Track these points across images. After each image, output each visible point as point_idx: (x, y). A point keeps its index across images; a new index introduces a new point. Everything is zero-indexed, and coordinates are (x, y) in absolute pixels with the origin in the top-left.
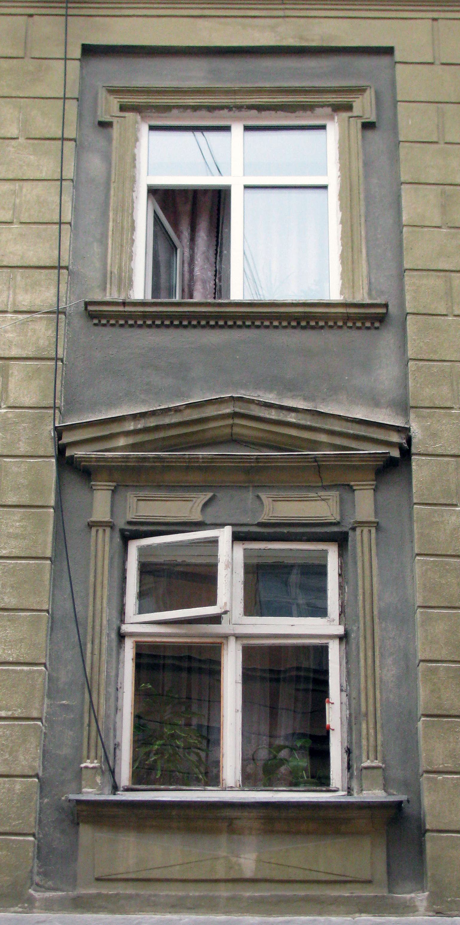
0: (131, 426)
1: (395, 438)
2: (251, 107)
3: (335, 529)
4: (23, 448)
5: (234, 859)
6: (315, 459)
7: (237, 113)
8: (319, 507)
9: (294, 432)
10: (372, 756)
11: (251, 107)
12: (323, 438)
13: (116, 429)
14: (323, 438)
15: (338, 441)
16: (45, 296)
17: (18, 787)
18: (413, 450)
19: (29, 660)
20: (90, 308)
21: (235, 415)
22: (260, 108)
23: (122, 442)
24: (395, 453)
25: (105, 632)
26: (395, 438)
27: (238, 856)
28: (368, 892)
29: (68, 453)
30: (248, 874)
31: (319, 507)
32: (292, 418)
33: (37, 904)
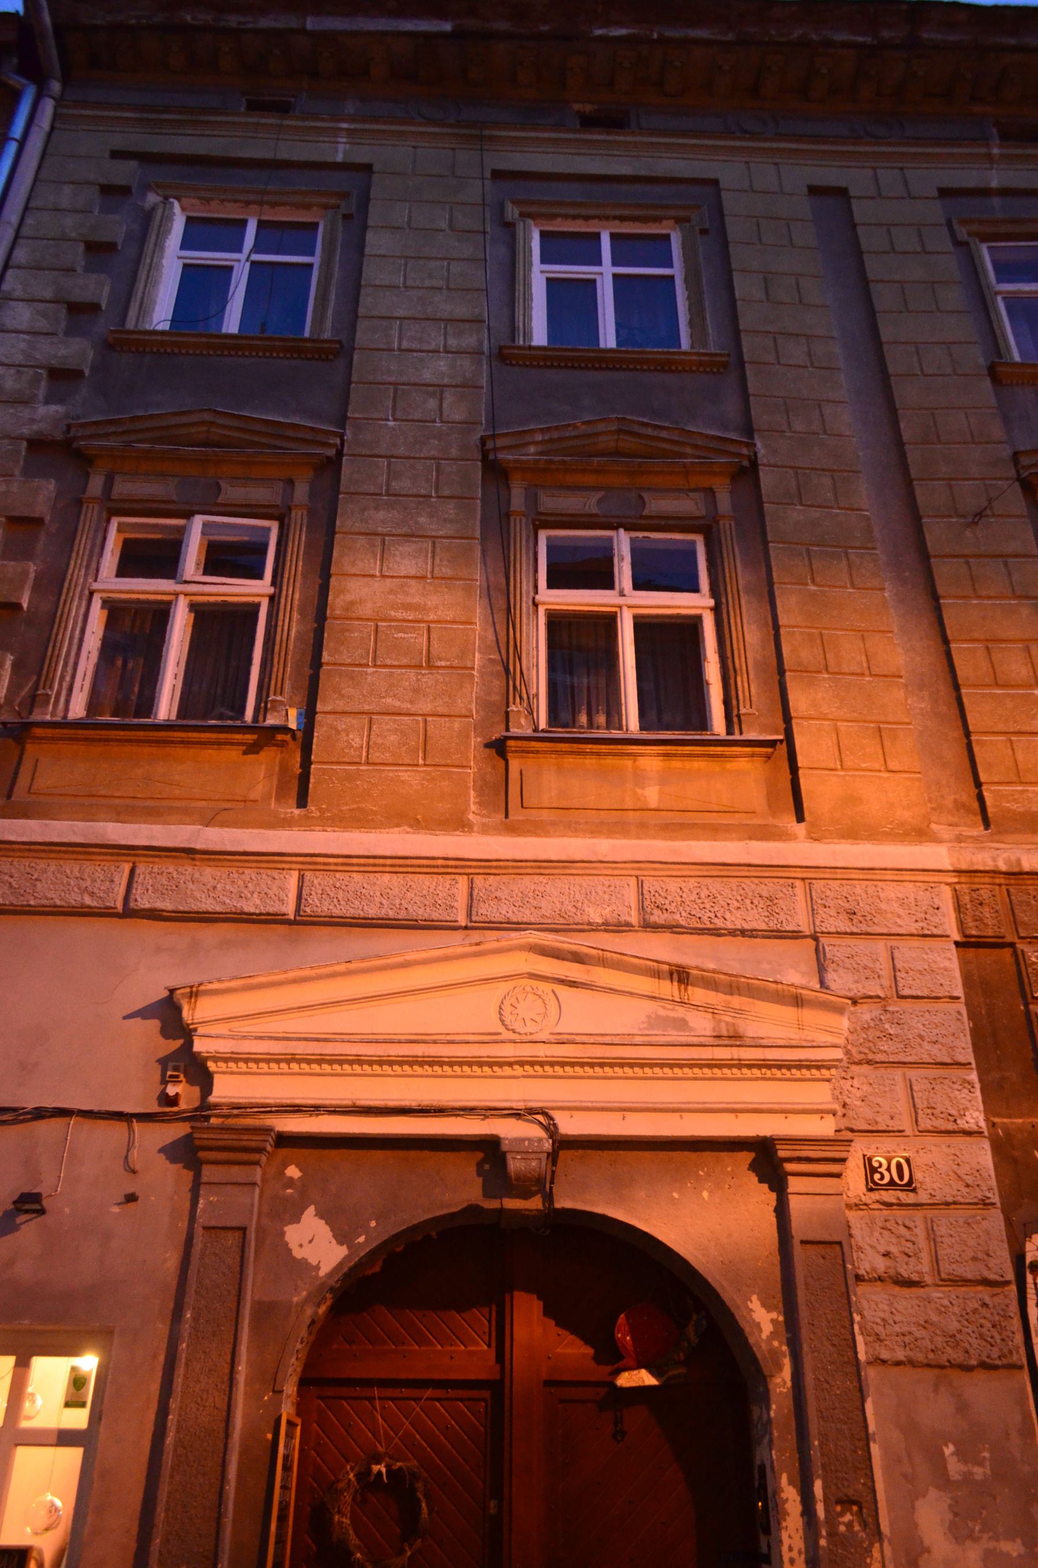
0: (539, 437)
2: (615, 218)
3: (702, 522)
4: (454, 452)
5: (639, 791)
6: (685, 466)
7: (605, 223)
9: (664, 446)
10: (748, 706)
16: (470, 341)
17: (456, 726)
18: (759, 462)
19: (463, 619)
20: (506, 351)
23: (532, 449)
25: (524, 599)
26: (745, 451)
27: (643, 788)
29: (491, 457)
30: (653, 804)
32: (664, 434)
33: (475, 829)
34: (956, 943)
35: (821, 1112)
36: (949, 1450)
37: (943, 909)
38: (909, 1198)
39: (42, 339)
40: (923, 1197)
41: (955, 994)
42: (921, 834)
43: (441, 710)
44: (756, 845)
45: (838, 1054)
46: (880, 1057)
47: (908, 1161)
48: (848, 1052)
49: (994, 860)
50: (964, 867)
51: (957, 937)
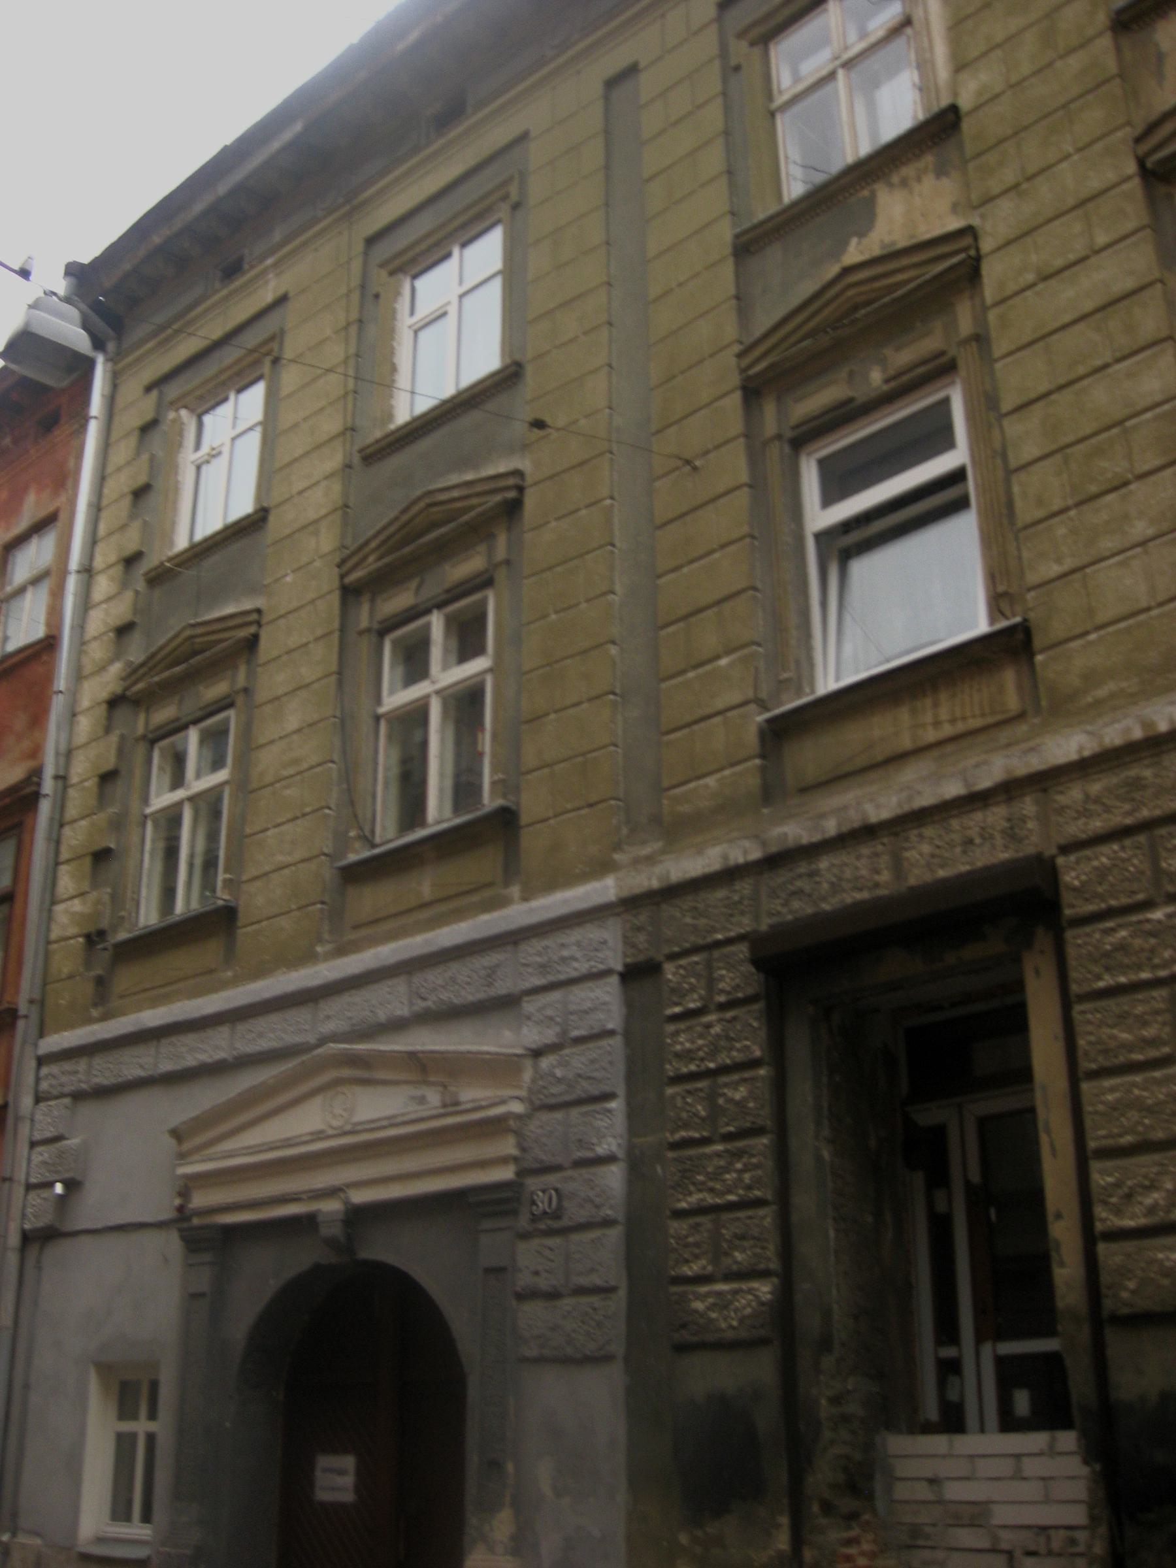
0: (373, 544)
1: (511, 481)
8: (469, 565)
9: (459, 505)
11: (457, 230)
13: (366, 550)
14: (474, 501)
23: (371, 559)
24: (512, 494)
28: (487, 893)
31: (469, 565)
35: (504, 1160)
37: (611, 943)
38: (556, 1225)
40: (565, 1222)
41: (610, 1026)
42: (603, 867)
44: (486, 917)
45: (517, 1108)
46: (552, 1101)
47: (556, 1190)
48: (531, 1102)
50: (626, 893)
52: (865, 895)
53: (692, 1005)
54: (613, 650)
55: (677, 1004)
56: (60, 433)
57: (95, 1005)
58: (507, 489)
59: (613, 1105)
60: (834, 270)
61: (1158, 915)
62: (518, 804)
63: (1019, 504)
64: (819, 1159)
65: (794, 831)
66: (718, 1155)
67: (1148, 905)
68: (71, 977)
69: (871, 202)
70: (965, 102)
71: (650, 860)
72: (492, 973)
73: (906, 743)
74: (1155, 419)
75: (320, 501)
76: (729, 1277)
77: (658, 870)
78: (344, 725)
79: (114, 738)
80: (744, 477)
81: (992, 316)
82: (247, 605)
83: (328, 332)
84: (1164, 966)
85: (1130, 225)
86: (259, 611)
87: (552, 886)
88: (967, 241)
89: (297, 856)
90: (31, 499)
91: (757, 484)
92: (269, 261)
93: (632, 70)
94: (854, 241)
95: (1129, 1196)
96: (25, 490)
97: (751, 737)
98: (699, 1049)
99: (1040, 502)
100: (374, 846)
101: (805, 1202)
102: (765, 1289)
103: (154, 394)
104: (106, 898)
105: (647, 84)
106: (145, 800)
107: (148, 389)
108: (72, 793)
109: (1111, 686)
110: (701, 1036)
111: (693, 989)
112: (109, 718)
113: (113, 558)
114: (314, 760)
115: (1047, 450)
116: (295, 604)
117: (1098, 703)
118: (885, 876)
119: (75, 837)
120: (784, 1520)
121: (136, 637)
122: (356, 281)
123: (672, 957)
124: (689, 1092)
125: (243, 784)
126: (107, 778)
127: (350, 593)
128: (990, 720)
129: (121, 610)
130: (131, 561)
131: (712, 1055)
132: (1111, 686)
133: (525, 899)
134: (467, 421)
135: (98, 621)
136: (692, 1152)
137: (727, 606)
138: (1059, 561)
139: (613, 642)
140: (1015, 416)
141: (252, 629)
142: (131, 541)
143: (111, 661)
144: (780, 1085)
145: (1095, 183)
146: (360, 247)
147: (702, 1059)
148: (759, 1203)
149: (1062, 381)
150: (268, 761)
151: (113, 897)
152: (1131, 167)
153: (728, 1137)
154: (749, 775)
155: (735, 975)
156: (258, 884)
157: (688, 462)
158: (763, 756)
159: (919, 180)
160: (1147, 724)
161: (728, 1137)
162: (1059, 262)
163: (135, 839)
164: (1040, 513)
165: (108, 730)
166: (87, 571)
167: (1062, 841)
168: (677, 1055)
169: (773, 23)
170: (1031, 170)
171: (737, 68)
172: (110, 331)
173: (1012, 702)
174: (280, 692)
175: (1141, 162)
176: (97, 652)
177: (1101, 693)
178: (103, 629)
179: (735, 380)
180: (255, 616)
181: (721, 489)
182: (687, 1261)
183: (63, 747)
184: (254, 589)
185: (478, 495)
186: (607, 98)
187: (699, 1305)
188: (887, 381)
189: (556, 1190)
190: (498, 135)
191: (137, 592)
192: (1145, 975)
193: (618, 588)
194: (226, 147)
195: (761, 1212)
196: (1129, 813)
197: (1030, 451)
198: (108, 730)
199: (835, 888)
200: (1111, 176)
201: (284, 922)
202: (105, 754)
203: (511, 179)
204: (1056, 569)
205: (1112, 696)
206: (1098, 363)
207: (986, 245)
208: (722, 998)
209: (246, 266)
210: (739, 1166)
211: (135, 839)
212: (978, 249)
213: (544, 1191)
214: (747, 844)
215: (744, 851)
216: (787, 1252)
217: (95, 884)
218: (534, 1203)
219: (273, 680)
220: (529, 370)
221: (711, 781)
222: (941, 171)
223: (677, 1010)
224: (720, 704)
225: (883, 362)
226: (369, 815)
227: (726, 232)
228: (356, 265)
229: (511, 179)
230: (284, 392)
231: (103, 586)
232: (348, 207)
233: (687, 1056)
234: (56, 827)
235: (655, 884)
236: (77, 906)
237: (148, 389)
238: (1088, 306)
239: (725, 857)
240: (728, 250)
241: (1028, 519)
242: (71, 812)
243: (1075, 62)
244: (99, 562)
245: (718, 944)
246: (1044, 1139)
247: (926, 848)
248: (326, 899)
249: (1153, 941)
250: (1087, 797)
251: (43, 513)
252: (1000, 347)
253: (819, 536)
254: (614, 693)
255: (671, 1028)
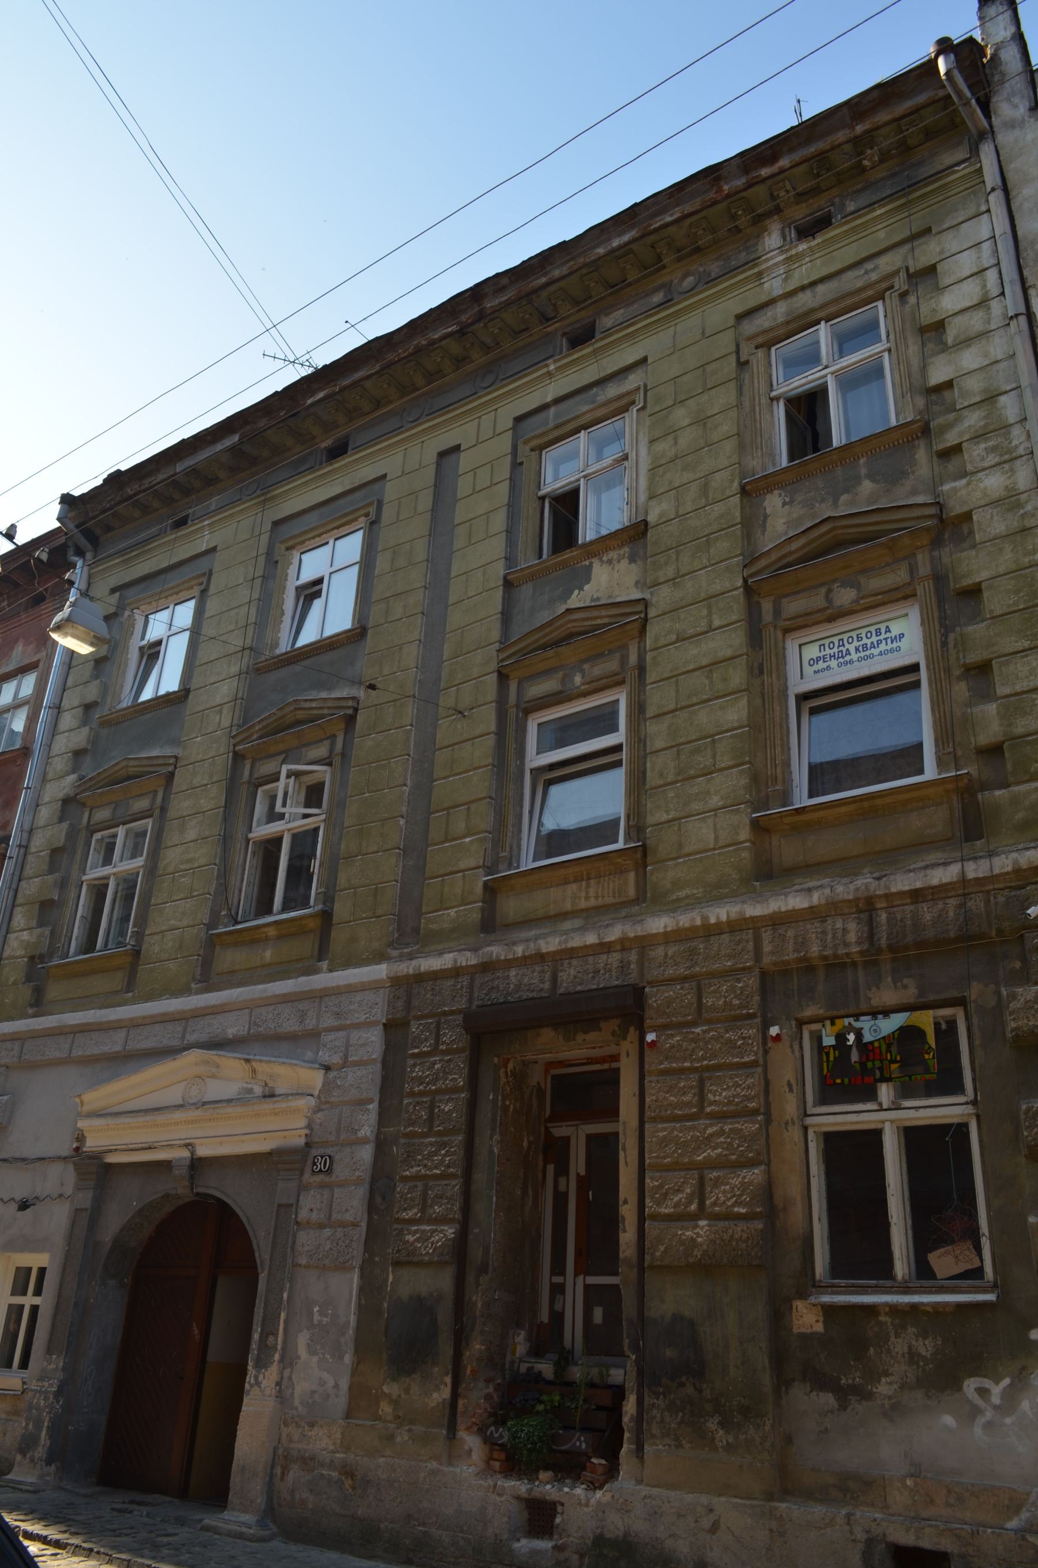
1: (350, 703)
2: (333, 529)
9: (315, 712)
12: (325, 711)
15: (331, 712)
16: (235, 669)
21: (296, 709)
22: (337, 528)
24: (350, 712)
34: (384, 1025)
36: (316, 1309)
39: (73, 733)
42: (380, 957)
43: (191, 923)
47: (330, 1157)
49: (408, 968)
51: (384, 1021)
52: (534, 995)
53: (425, 1049)
54: (402, 822)
55: (415, 1047)
56: (45, 607)
57: (31, 1006)
58: (348, 707)
59: (371, 1106)
60: (562, 609)
61: (698, 1030)
62: (332, 909)
63: (648, 774)
64: (491, 1152)
65: (496, 951)
66: (431, 1144)
67: (694, 1024)
68: (15, 983)
69: (590, 567)
70: (652, 518)
71: (411, 957)
72: (303, 1016)
73: (568, 906)
74: (731, 737)
75: (225, 691)
76: (430, 1221)
77: (414, 963)
78: (226, 841)
79: (65, 825)
80: (493, 727)
81: (649, 657)
82: (168, 751)
83: (241, 580)
84: (698, 1060)
85: (735, 618)
86: (176, 757)
87: (348, 964)
88: (640, 607)
89: (185, 923)
90: (19, 648)
91: (501, 733)
92: (206, 523)
93: (457, 448)
94: (576, 592)
95: (666, 1194)
96: (16, 641)
97: (479, 889)
98: (427, 1076)
99: (661, 775)
100: (237, 923)
101: (480, 1177)
102: (450, 1231)
103: (117, 594)
104: (47, 933)
105: (465, 461)
106: (84, 872)
107: (113, 591)
108: (30, 858)
109: (687, 891)
110: (428, 1069)
111: (426, 1040)
112: (63, 811)
113: (76, 703)
114: (202, 861)
115: (669, 745)
116: (200, 757)
117: (678, 900)
118: (547, 985)
119: (30, 888)
120: (448, 1380)
121: (88, 760)
122: (262, 550)
123: (418, 1018)
124: (418, 1103)
125: (152, 869)
126: (55, 852)
127: (238, 757)
128: (617, 900)
129: (80, 738)
130: (88, 708)
131: (434, 1082)
132: (687, 891)
133: (331, 971)
134: (326, 657)
135: (63, 744)
136: (416, 1141)
137: (473, 806)
138: (667, 812)
139: (402, 817)
140: (654, 720)
141: (171, 769)
142: (92, 692)
143: (68, 774)
144: (472, 1105)
145: (717, 587)
146: (269, 526)
147: (428, 1084)
148: (453, 1176)
149: (683, 704)
150: (171, 857)
151: (52, 933)
152: (740, 583)
153: (439, 1134)
154: (473, 912)
155: (452, 1035)
156: (156, 937)
157: (460, 712)
158: (483, 901)
159: (619, 562)
160: (705, 918)
161: (439, 1134)
162: (691, 632)
163: (73, 895)
164: (661, 782)
165: (61, 820)
166: (58, 708)
167: (650, 979)
168: (413, 1078)
169: (545, 439)
170: (683, 571)
171: (521, 464)
172: (89, 546)
173: (632, 892)
174: (185, 814)
175: (745, 581)
176: (59, 764)
177: (682, 894)
178: (63, 750)
179: (494, 666)
180: (172, 761)
181: (478, 732)
182: (405, 1209)
183: (27, 826)
184: (175, 742)
185: (329, 708)
186: (438, 464)
187: (410, 1238)
188: (583, 684)
189: (330, 1157)
190: (367, 472)
191: (91, 729)
192: (687, 1064)
193: (408, 782)
194: (184, 440)
195: (454, 1182)
196: (689, 968)
197: (659, 743)
198: (61, 820)
199: (518, 988)
200: (728, 585)
201: (172, 965)
202: (58, 834)
203: (371, 503)
204: (665, 817)
205: (687, 897)
206: (705, 697)
207: (652, 613)
208: (443, 1047)
209: (190, 523)
210: (443, 1152)
211: (73, 895)
212: (646, 614)
213: (322, 1157)
214: (468, 954)
215: (468, 959)
216: (466, 1208)
217: (41, 924)
218: (314, 1164)
219: (181, 805)
220: (370, 632)
221: (452, 912)
222: (632, 559)
223: (416, 1051)
224: (462, 865)
225: (582, 671)
226: (235, 902)
227: (499, 569)
228: (265, 539)
229: (371, 503)
230: (207, 615)
231: (67, 720)
232: (263, 498)
233: (420, 1080)
234: (16, 879)
235: (411, 971)
236: (25, 936)
237: (113, 591)
238: (704, 662)
239: (455, 961)
240: (501, 582)
241: (653, 784)
242: (28, 871)
243: (718, 509)
244: (66, 704)
245: (445, 1013)
246: (622, 1154)
247: (572, 972)
248: (201, 953)
249: (694, 1045)
250: (666, 955)
251: (26, 661)
252: (651, 676)
253: (531, 770)
254: (399, 848)
255: (410, 1062)
